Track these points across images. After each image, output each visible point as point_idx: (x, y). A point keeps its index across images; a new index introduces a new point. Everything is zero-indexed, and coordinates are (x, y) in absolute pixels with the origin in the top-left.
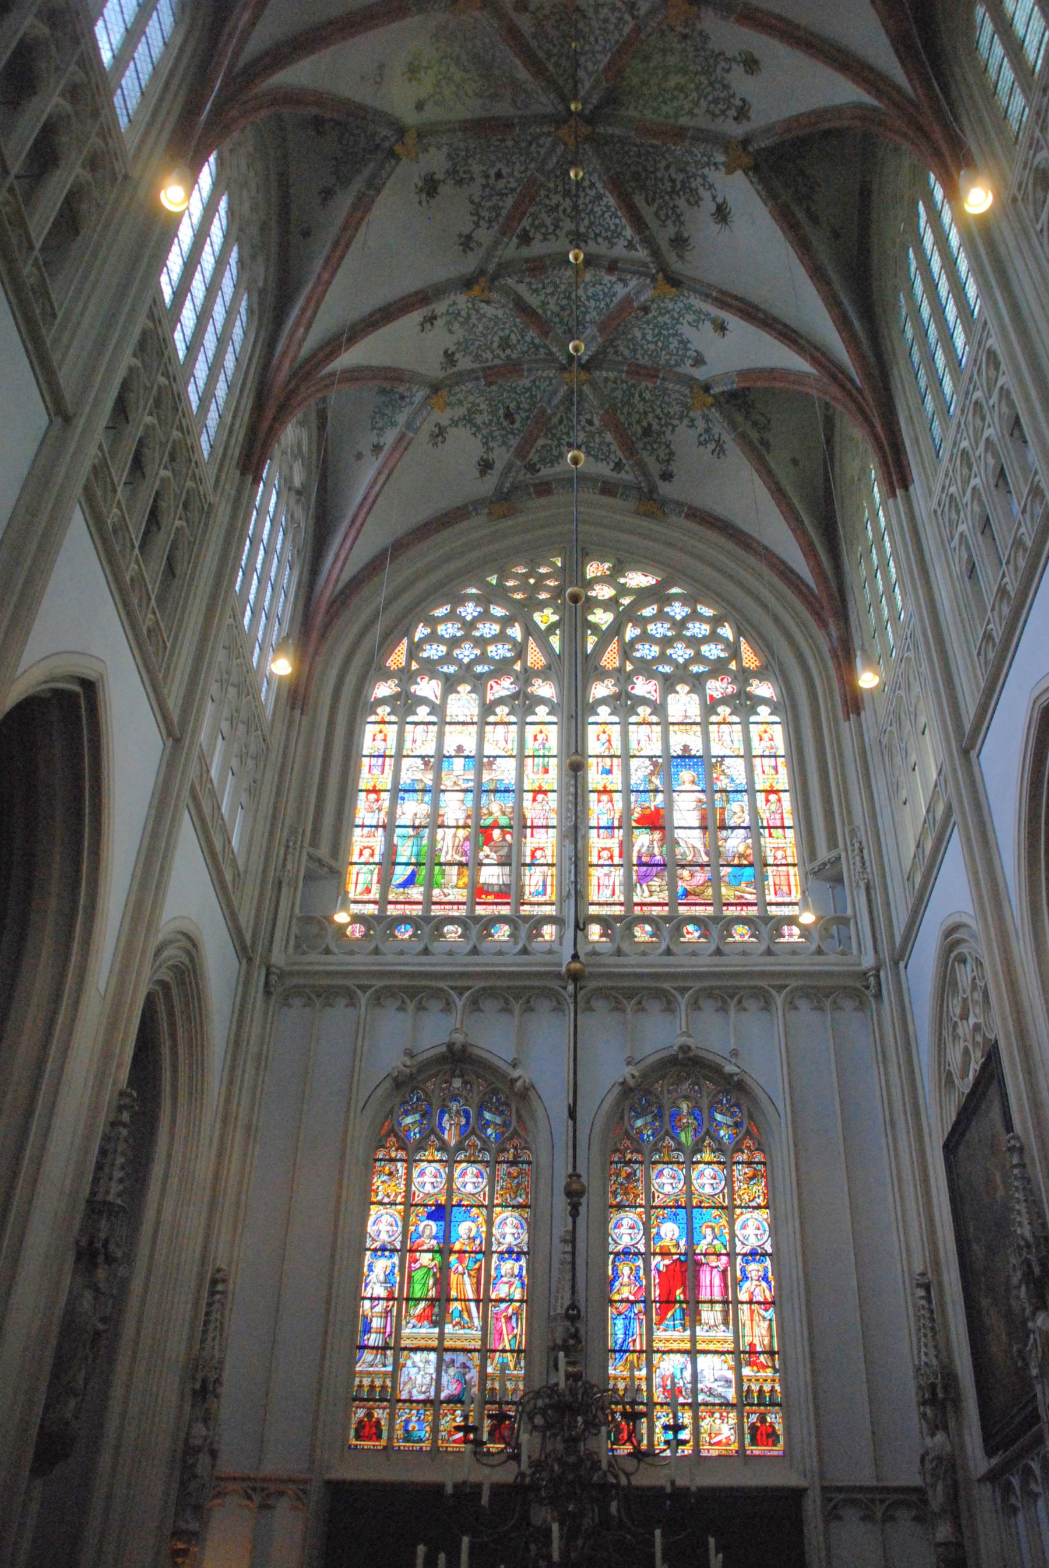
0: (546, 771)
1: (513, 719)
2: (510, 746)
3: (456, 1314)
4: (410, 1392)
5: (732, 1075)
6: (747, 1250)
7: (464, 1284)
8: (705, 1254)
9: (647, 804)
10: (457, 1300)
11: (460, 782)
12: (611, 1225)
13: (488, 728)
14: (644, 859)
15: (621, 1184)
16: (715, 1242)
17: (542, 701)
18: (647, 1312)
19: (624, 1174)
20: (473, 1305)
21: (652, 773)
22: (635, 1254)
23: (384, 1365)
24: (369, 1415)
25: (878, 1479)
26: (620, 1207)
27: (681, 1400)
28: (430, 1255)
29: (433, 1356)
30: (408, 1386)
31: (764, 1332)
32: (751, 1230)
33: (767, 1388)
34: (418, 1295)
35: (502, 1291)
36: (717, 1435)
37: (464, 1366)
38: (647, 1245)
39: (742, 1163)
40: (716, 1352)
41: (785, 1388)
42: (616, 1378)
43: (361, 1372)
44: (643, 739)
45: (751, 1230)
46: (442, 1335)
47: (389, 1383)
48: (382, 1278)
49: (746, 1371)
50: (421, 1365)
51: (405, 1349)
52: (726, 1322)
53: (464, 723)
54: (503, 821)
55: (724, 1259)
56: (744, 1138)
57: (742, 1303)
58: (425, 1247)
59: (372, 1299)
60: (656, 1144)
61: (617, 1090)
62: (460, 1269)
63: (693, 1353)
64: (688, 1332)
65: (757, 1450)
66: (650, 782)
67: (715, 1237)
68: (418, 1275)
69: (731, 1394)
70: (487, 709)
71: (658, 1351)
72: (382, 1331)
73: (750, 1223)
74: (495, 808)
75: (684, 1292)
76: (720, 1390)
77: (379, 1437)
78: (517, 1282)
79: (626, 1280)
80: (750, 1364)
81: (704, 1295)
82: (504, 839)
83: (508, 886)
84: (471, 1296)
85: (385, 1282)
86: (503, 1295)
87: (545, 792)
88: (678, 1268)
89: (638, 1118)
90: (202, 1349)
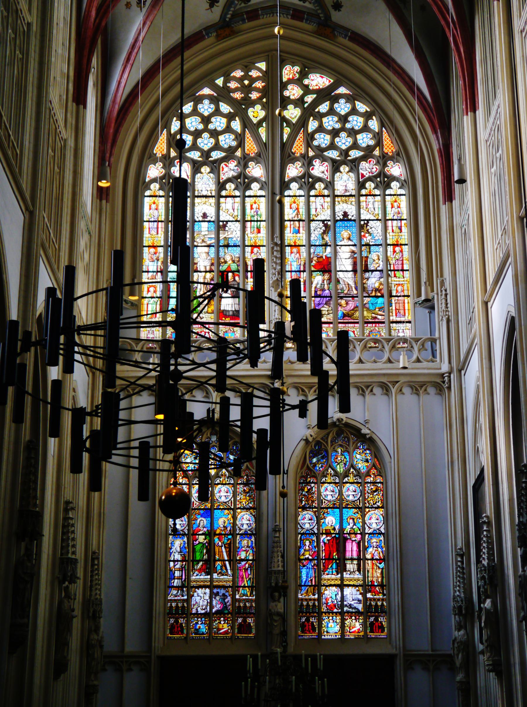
0: (259, 232)
1: (237, 193)
2: (236, 213)
3: (219, 568)
4: (197, 609)
5: (366, 434)
6: (371, 531)
7: (222, 552)
8: (350, 534)
9: (321, 254)
10: (219, 560)
11: (206, 240)
12: (299, 518)
13: (222, 200)
14: (318, 293)
15: (305, 495)
16: (355, 527)
17: (255, 180)
18: (318, 565)
19: (306, 490)
20: (227, 563)
21: (324, 232)
22: (312, 534)
23: (183, 596)
24: (176, 621)
25: (432, 651)
26: (304, 508)
27: (335, 610)
28: (203, 537)
29: (208, 591)
30: (196, 606)
31: (379, 575)
32: (373, 521)
33: (379, 603)
34: (198, 558)
35: (243, 555)
36: (353, 628)
37: (224, 595)
38: (318, 529)
39: (370, 483)
40: (353, 586)
41: (389, 604)
42: (302, 600)
43: (171, 600)
44: (319, 207)
45: (373, 521)
46: (212, 579)
47: (185, 605)
48: (179, 549)
49: (369, 595)
50: (202, 595)
51: (193, 587)
52: (359, 570)
53: (206, 197)
54: (234, 267)
55: (359, 536)
56: (372, 468)
57: (368, 560)
58: (201, 533)
59: (174, 561)
60: (323, 473)
61: (303, 443)
62: (220, 544)
63: (341, 586)
64: (339, 575)
65: (373, 635)
66: (323, 238)
67: (355, 524)
68: (198, 548)
69: (360, 607)
70: (221, 186)
71: (324, 585)
72: (180, 578)
73: (373, 516)
74: (228, 258)
75: (337, 554)
76: (355, 605)
77: (182, 633)
78: (250, 551)
79: (307, 548)
80: (370, 592)
81: (348, 555)
82: (234, 280)
83: (238, 311)
84: (226, 558)
85: (181, 552)
86: (243, 557)
87: (258, 247)
88: (335, 542)
89: (314, 457)
90: (91, 595)
